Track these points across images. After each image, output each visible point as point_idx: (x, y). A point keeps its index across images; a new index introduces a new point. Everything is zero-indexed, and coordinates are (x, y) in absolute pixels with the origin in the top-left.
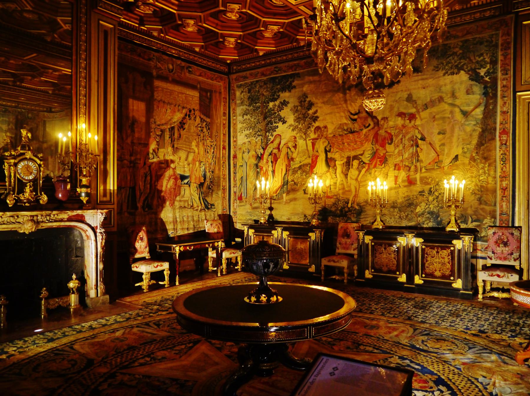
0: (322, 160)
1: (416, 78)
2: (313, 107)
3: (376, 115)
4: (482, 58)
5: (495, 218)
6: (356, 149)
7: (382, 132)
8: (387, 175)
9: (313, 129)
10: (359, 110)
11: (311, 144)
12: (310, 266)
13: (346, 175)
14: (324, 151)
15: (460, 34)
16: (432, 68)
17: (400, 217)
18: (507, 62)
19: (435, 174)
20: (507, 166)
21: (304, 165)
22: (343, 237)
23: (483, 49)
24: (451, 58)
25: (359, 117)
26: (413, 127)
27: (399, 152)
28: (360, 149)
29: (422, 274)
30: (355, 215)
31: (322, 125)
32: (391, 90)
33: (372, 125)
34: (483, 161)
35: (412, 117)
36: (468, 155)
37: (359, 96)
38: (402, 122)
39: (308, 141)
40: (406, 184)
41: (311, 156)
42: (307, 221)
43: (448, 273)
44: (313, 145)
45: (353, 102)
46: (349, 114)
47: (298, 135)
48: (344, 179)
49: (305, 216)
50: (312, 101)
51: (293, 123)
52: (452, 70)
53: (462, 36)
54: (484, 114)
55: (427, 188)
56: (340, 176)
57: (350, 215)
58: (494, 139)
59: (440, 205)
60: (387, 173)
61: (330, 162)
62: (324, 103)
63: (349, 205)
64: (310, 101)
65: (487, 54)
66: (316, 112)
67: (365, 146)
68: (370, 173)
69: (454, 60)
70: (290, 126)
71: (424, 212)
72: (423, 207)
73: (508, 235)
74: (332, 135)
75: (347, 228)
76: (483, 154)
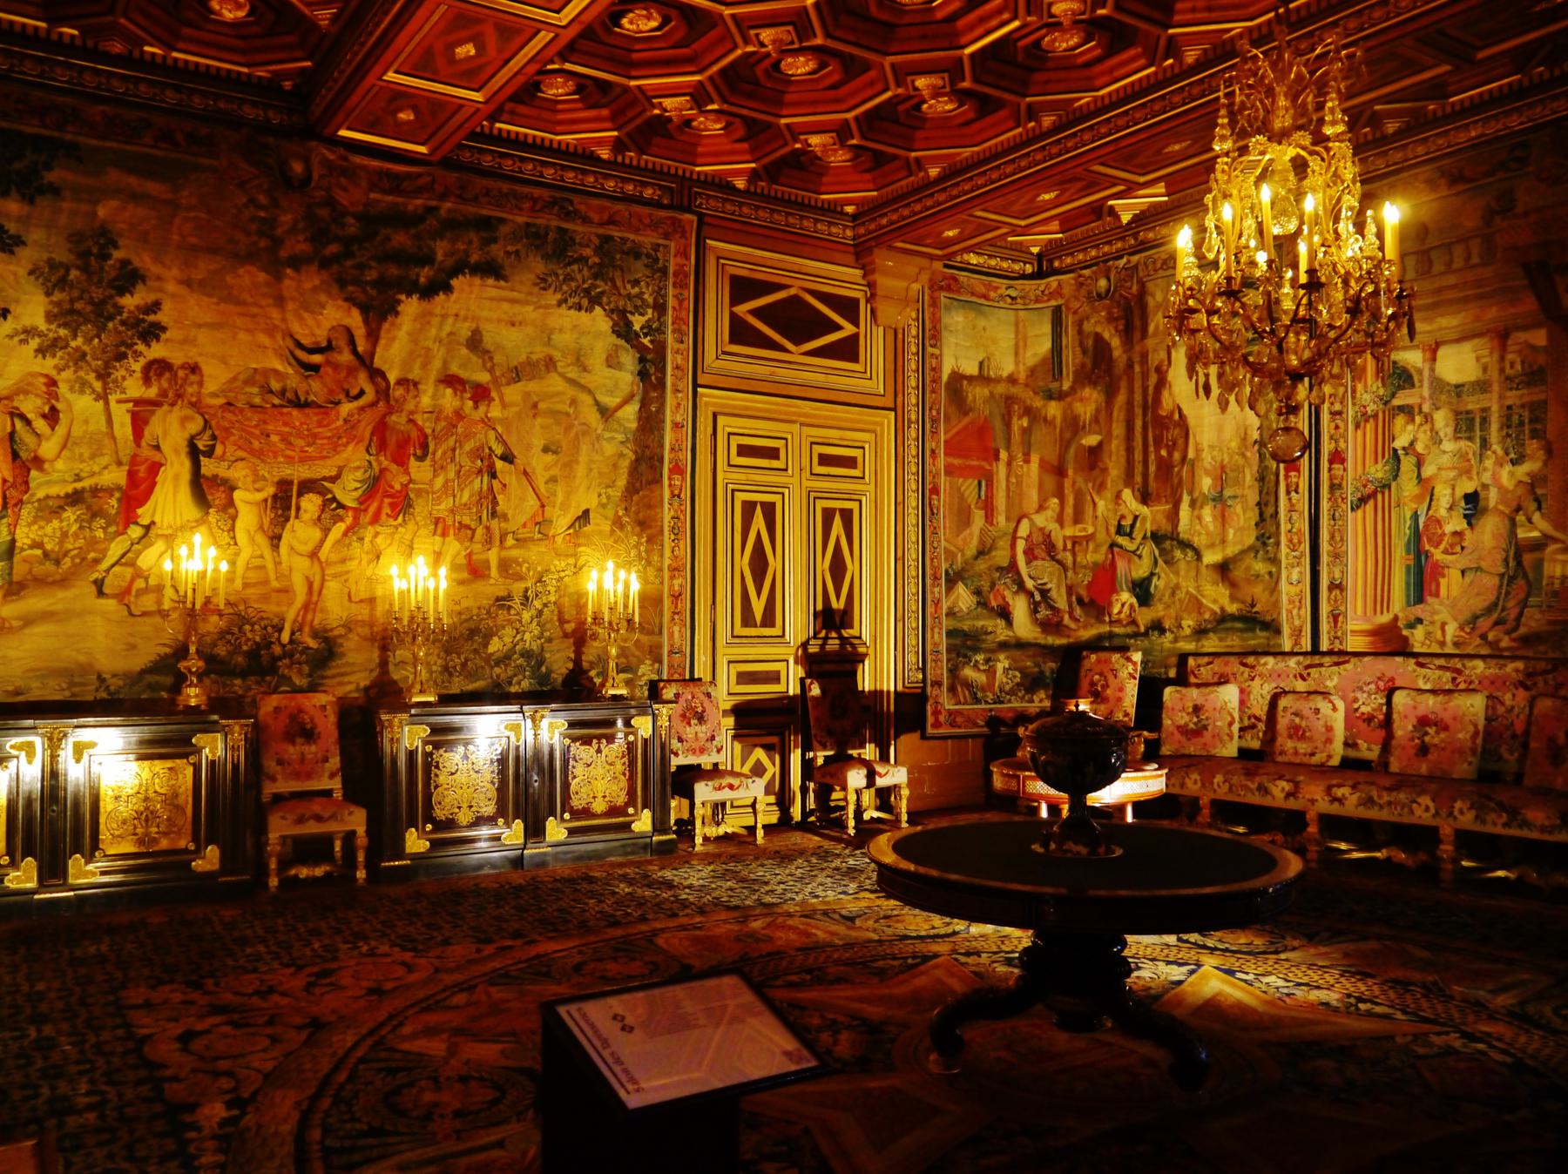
0: (176, 478)
1: (494, 293)
2: (140, 287)
3: (384, 368)
4: (637, 290)
5: (661, 662)
6: (310, 458)
7: (398, 420)
8: (411, 547)
9: (137, 367)
10: (329, 341)
11: (128, 419)
12: (198, 853)
13: (275, 540)
14: (184, 450)
15: (596, 218)
16: (532, 277)
17: (446, 668)
18: (684, 314)
19: (534, 555)
20: (682, 544)
21: (96, 491)
22: (289, 737)
23: (639, 269)
24: (575, 267)
25: (328, 362)
26: (482, 421)
27: (447, 481)
28: (329, 462)
29: (563, 812)
30: (306, 669)
31: (177, 357)
32: (425, 304)
33: (370, 396)
34: (637, 529)
35: (481, 394)
36: (610, 513)
37: (329, 295)
38: (457, 403)
39: (113, 405)
40: (465, 575)
41: (125, 459)
42: (104, 695)
43: (621, 799)
44: (139, 424)
45: (307, 309)
46: (290, 343)
47: (68, 374)
48: (267, 552)
49: (101, 679)
50: (137, 263)
51: (42, 326)
52: (576, 300)
53: (602, 224)
54: (640, 419)
55: (518, 588)
56: (252, 540)
57: (289, 667)
58: (659, 481)
59: (547, 634)
60: (412, 541)
61: (204, 490)
62: (187, 283)
63: (285, 637)
64: (125, 263)
65: (648, 285)
66: (155, 307)
67: (345, 455)
68: (361, 539)
69: (582, 275)
70: (26, 331)
71: (512, 651)
72: (508, 640)
73: (702, 697)
74: (221, 401)
75: (301, 710)
76: (637, 513)
